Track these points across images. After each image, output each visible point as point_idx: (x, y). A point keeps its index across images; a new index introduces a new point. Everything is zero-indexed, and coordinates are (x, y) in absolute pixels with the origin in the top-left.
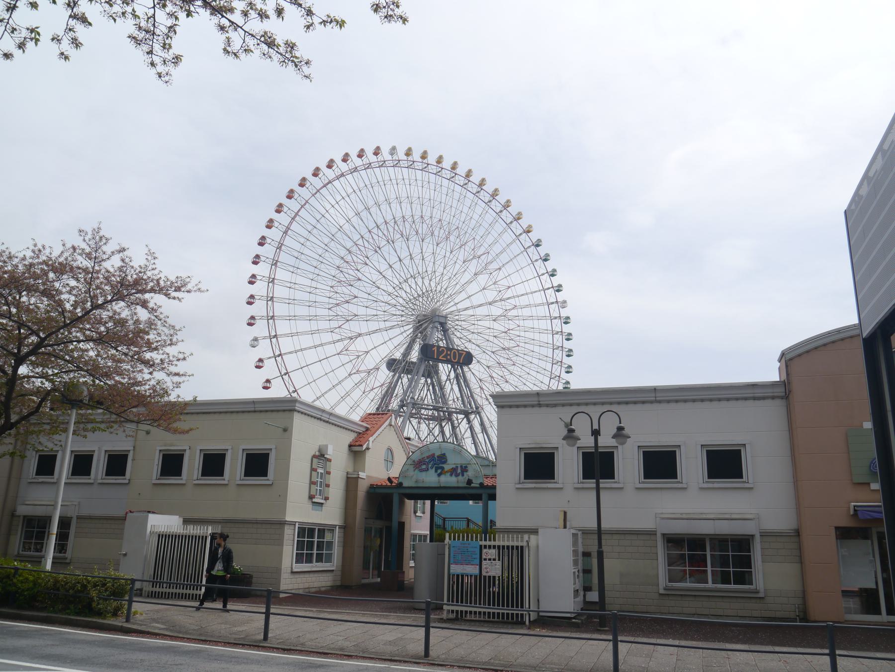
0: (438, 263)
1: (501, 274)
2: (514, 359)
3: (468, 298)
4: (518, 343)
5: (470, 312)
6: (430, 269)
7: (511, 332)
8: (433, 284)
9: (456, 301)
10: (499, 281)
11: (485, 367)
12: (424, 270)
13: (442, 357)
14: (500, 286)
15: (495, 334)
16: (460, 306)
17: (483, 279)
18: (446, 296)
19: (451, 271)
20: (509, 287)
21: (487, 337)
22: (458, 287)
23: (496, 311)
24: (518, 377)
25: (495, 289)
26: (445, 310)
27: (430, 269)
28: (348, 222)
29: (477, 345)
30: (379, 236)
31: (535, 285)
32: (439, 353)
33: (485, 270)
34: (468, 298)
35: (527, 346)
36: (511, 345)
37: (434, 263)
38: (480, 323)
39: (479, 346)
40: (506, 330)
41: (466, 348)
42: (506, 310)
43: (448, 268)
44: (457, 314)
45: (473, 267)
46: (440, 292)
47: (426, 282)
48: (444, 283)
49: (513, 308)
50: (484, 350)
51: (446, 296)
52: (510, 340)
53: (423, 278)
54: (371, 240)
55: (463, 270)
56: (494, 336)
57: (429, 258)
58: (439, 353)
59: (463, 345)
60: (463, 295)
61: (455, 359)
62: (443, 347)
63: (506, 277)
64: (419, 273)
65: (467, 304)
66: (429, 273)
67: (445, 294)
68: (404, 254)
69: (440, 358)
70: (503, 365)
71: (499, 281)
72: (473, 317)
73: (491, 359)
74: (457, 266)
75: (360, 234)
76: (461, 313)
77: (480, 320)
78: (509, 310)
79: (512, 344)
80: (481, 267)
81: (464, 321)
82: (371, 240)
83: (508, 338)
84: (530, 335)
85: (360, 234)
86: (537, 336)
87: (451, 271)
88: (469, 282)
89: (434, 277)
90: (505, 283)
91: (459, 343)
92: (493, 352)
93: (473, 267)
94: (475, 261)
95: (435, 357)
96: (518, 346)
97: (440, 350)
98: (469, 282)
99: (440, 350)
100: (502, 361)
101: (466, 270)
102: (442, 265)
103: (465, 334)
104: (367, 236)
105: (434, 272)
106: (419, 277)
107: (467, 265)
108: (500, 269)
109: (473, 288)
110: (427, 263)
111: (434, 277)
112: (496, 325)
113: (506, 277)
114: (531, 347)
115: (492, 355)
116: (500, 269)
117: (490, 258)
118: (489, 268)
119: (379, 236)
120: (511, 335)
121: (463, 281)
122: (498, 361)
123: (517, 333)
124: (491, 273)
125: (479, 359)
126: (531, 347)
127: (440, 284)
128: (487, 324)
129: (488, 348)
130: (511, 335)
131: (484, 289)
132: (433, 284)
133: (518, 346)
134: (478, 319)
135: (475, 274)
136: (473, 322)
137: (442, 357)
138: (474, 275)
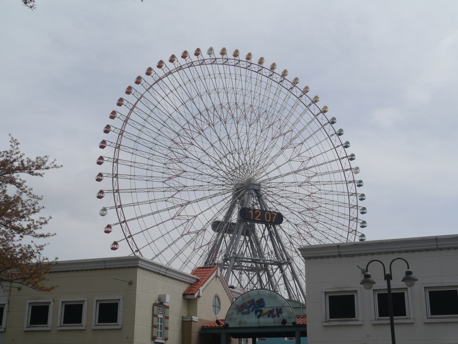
0: (251, 141)
1: (304, 148)
2: (317, 217)
3: (277, 168)
4: (320, 204)
6: (244, 146)
7: (314, 195)
8: (248, 159)
9: (267, 171)
10: (302, 153)
11: (294, 225)
12: (240, 147)
13: (257, 218)
14: (303, 158)
15: (301, 198)
16: (270, 176)
17: (288, 152)
18: (259, 168)
19: (262, 147)
20: (311, 158)
21: (294, 200)
22: (268, 159)
25: (299, 160)
26: (259, 179)
27: (244, 146)
28: (176, 110)
29: (286, 207)
30: (201, 121)
31: (332, 155)
32: (255, 215)
33: (290, 144)
34: (277, 168)
36: (314, 206)
37: (248, 141)
38: (287, 189)
39: (288, 208)
40: (310, 193)
41: (277, 210)
43: (259, 145)
44: (268, 182)
45: (280, 142)
46: (254, 164)
47: (242, 157)
48: (256, 157)
51: (259, 168)
52: (313, 201)
53: (239, 154)
54: (195, 125)
55: (272, 145)
56: (300, 199)
57: (243, 137)
58: (255, 215)
59: (274, 208)
60: (273, 166)
61: (268, 219)
62: (258, 210)
63: (307, 150)
64: (235, 150)
65: (276, 173)
66: (244, 149)
67: (257, 166)
68: (223, 135)
69: (256, 219)
71: (302, 153)
72: (282, 184)
74: (267, 143)
75: (187, 120)
76: (272, 181)
77: (287, 186)
79: (315, 205)
80: (287, 143)
81: (274, 187)
82: (195, 125)
83: (312, 200)
84: (329, 197)
85: (187, 120)
86: (335, 198)
87: (262, 147)
88: (277, 155)
89: (248, 152)
90: (307, 154)
91: (271, 206)
92: (300, 213)
93: (280, 142)
94: (281, 138)
95: (252, 219)
96: (320, 206)
97: (256, 212)
98: (277, 155)
99: (256, 212)
101: (274, 146)
102: (255, 142)
103: (276, 199)
104: (192, 121)
105: (248, 148)
106: (236, 153)
107: (275, 142)
108: (302, 143)
109: (280, 160)
110: (242, 141)
111: (248, 152)
112: (301, 190)
113: (307, 150)
116: (302, 143)
118: (293, 143)
119: (201, 121)
120: (314, 198)
121: (272, 155)
123: (319, 196)
124: (295, 147)
125: (288, 219)
127: (254, 158)
128: (294, 189)
130: (314, 198)
131: (290, 160)
132: (248, 159)
133: (320, 206)
134: (286, 185)
136: (282, 188)
137: (257, 218)
138: (281, 149)
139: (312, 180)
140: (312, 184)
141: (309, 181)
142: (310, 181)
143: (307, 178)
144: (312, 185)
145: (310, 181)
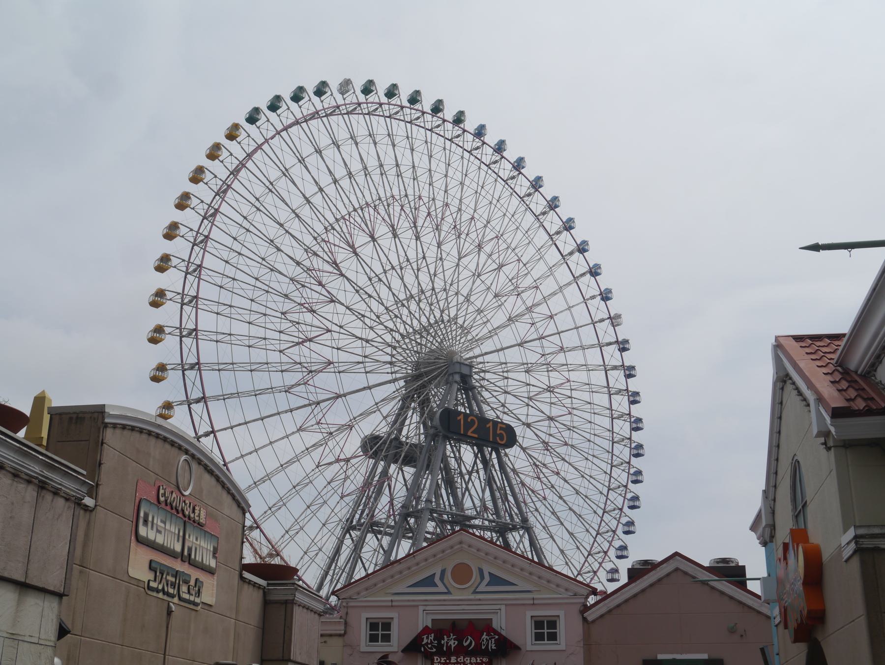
5: (374, 379)
23: (327, 382)
24: (270, 290)
35: (261, 333)
42: (305, 384)
49: (293, 386)
50: (342, 331)
70: (305, 310)
73: (329, 317)
78: (299, 385)
88: (366, 414)
98: (366, 414)
100: (308, 317)
114: (255, 331)
115: (329, 325)
117: (316, 454)
122: (314, 314)
126: (255, 331)
129: (336, 335)
135: (351, 427)
139: (299, 376)
140: (299, 366)
141: (308, 374)
142: (305, 374)
143: (311, 382)
144: (300, 363)
145: (305, 374)
